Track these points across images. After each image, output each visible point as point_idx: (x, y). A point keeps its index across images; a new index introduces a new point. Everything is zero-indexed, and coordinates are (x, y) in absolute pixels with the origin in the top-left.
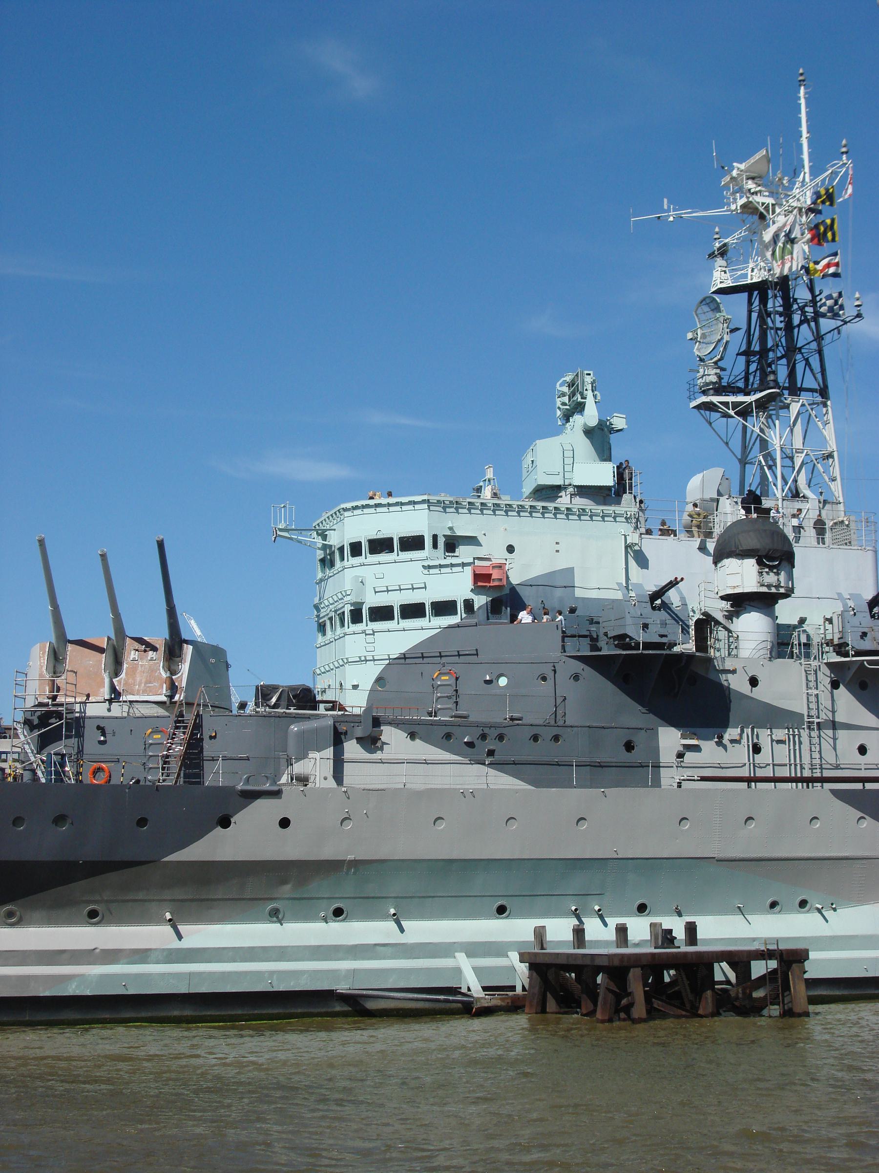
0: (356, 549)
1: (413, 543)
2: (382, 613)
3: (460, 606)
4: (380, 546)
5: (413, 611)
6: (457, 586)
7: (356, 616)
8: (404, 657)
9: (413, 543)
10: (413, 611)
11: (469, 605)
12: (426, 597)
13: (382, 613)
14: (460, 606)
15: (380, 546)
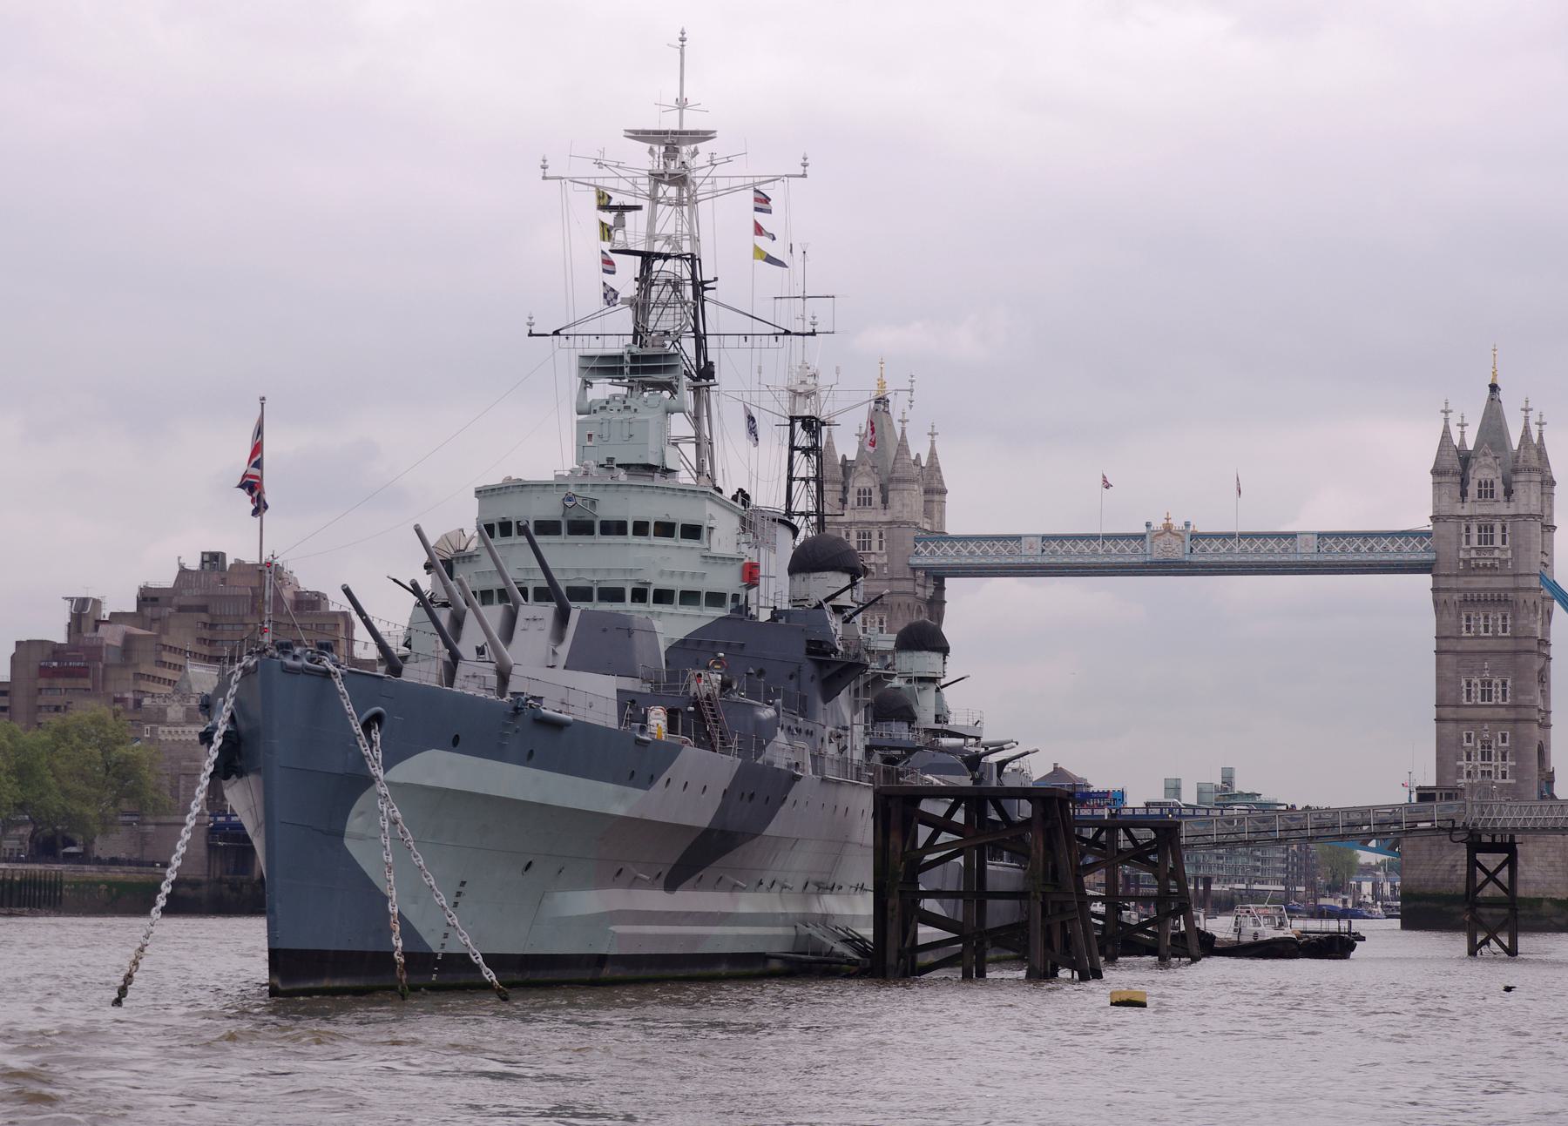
0: (641, 528)
1: (692, 532)
2: (663, 596)
3: (729, 598)
4: (665, 529)
5: (690, 597)
6: (727, 581)
7: (639, 595)
8: (683, 642)
9: (692, 532)
10: (690, 597)
11: (736, 597)
12: (704, 586)
13: (663, 596)
14: (729, 598)
15: (665, 529)
